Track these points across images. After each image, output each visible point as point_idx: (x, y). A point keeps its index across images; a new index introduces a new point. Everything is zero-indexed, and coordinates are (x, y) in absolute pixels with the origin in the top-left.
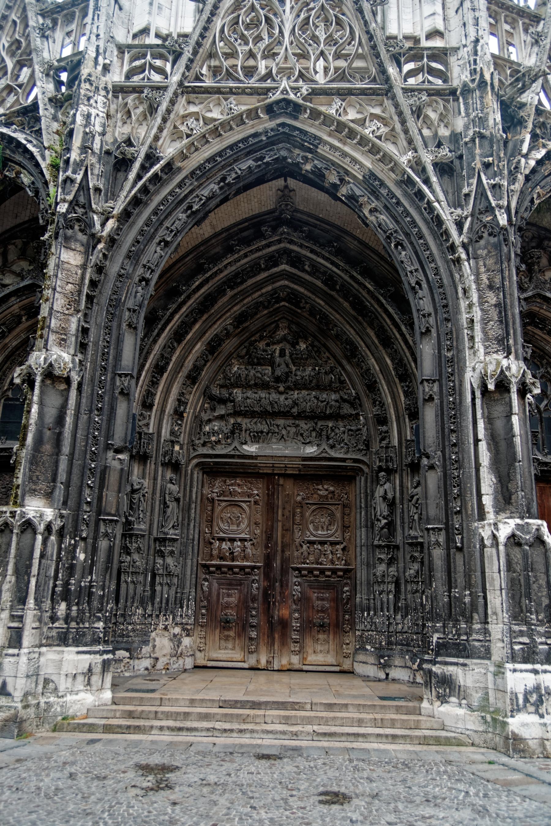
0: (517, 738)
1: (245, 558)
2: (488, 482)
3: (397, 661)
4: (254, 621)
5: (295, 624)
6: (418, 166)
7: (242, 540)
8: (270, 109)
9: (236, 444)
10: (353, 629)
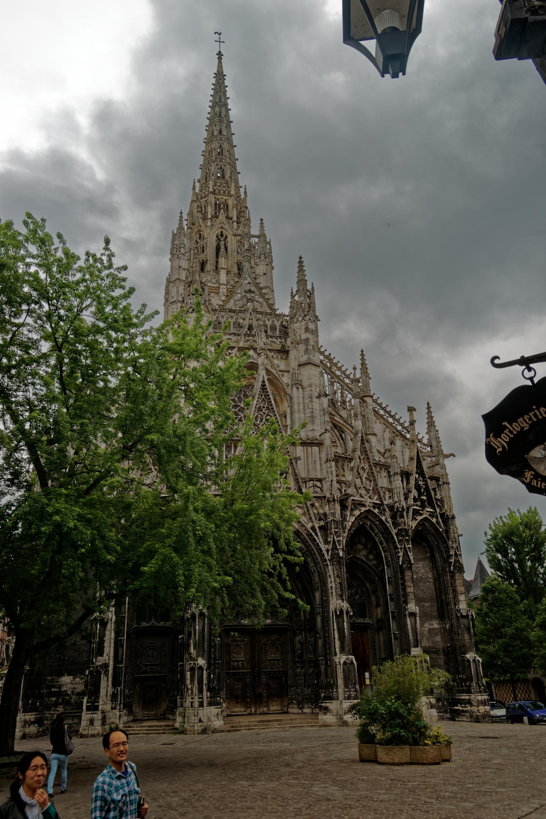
0: (346, 722)
1: (244, 668)
2: (337, 644)
3: (306, 706)
4: (248, 695)
5: (265, 695)
6: (313, 528)
7: (242, 661)
9: (239, 620)
10: (287, 695)
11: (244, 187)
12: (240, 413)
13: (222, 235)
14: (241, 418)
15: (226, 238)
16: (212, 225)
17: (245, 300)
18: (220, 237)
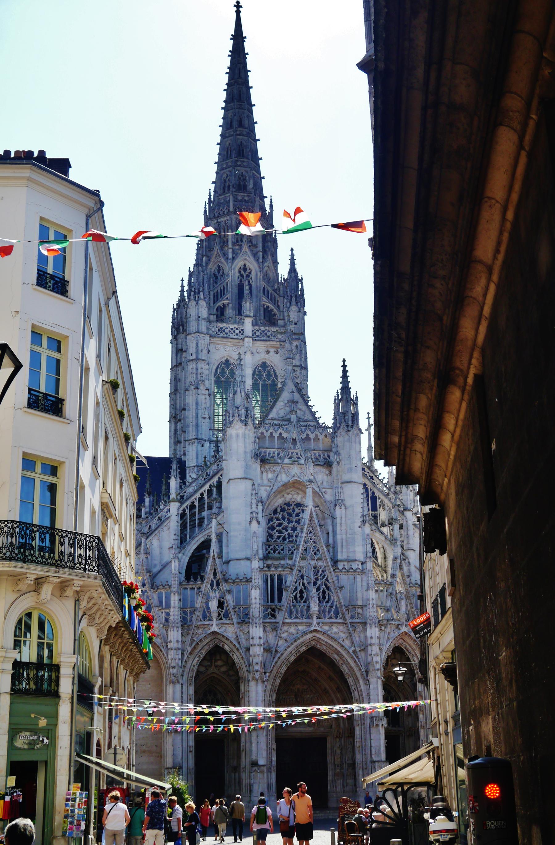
8: (311, 632)
11: (269, 198)
12: (284, 531)
13: (245, 269)
14: (284, 536)
15: (250, 273)
16: (233, 258)
17: (288, 409)
18: (242, 272)
